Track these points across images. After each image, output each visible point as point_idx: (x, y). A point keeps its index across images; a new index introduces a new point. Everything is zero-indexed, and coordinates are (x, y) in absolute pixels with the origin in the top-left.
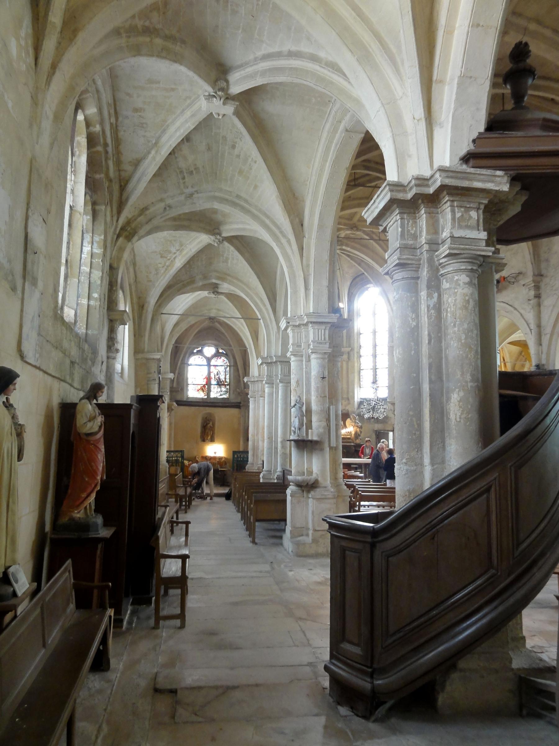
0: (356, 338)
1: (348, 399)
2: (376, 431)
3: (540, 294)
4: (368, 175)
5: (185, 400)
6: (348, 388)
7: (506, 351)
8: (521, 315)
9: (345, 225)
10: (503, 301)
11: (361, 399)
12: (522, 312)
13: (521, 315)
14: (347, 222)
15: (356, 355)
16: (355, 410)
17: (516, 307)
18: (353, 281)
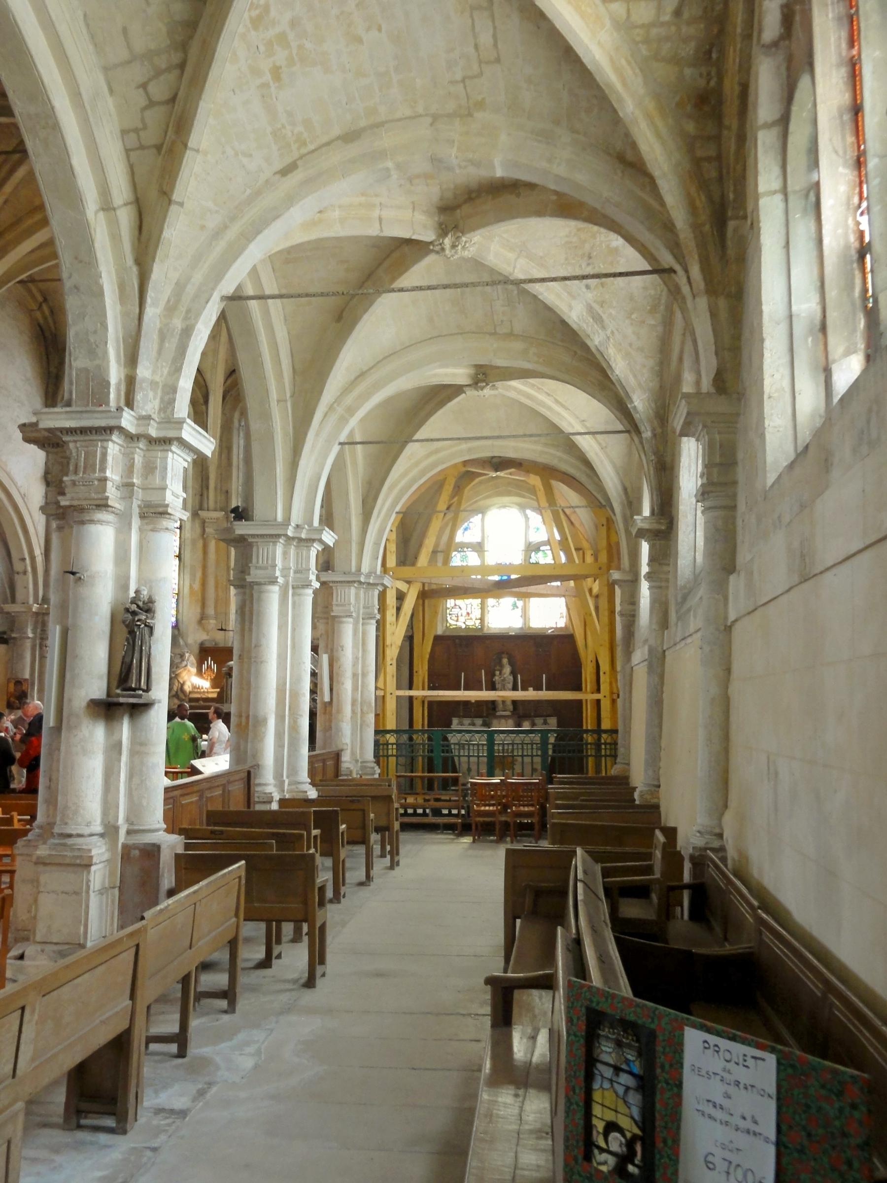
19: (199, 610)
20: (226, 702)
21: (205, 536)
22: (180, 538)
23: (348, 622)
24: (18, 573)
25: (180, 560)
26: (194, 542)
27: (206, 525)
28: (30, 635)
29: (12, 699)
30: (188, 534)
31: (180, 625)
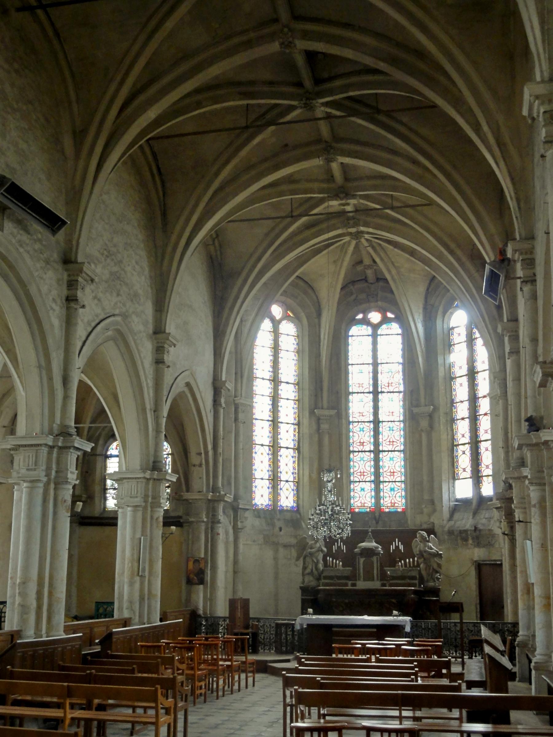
0: (442, 388)
1: (432, 502)
2: (476, 561)
3: (535, 275)
4: (276, 105)
5: (97, 515)
6: (431, 480)
11: (457, 500)
14: (325, 185)
15: (443, 420)
16: (445, 522)
18: (430, 284)
20: (359, 580)
21: (321, 431)
22: (299, 433)
24: (194, 466)
25: (299, 453)
26: (311, 436)
27: (321, 421)
28: (205, 520)
29: (192, 576)
30: (306, 430)
31: (301, 510)
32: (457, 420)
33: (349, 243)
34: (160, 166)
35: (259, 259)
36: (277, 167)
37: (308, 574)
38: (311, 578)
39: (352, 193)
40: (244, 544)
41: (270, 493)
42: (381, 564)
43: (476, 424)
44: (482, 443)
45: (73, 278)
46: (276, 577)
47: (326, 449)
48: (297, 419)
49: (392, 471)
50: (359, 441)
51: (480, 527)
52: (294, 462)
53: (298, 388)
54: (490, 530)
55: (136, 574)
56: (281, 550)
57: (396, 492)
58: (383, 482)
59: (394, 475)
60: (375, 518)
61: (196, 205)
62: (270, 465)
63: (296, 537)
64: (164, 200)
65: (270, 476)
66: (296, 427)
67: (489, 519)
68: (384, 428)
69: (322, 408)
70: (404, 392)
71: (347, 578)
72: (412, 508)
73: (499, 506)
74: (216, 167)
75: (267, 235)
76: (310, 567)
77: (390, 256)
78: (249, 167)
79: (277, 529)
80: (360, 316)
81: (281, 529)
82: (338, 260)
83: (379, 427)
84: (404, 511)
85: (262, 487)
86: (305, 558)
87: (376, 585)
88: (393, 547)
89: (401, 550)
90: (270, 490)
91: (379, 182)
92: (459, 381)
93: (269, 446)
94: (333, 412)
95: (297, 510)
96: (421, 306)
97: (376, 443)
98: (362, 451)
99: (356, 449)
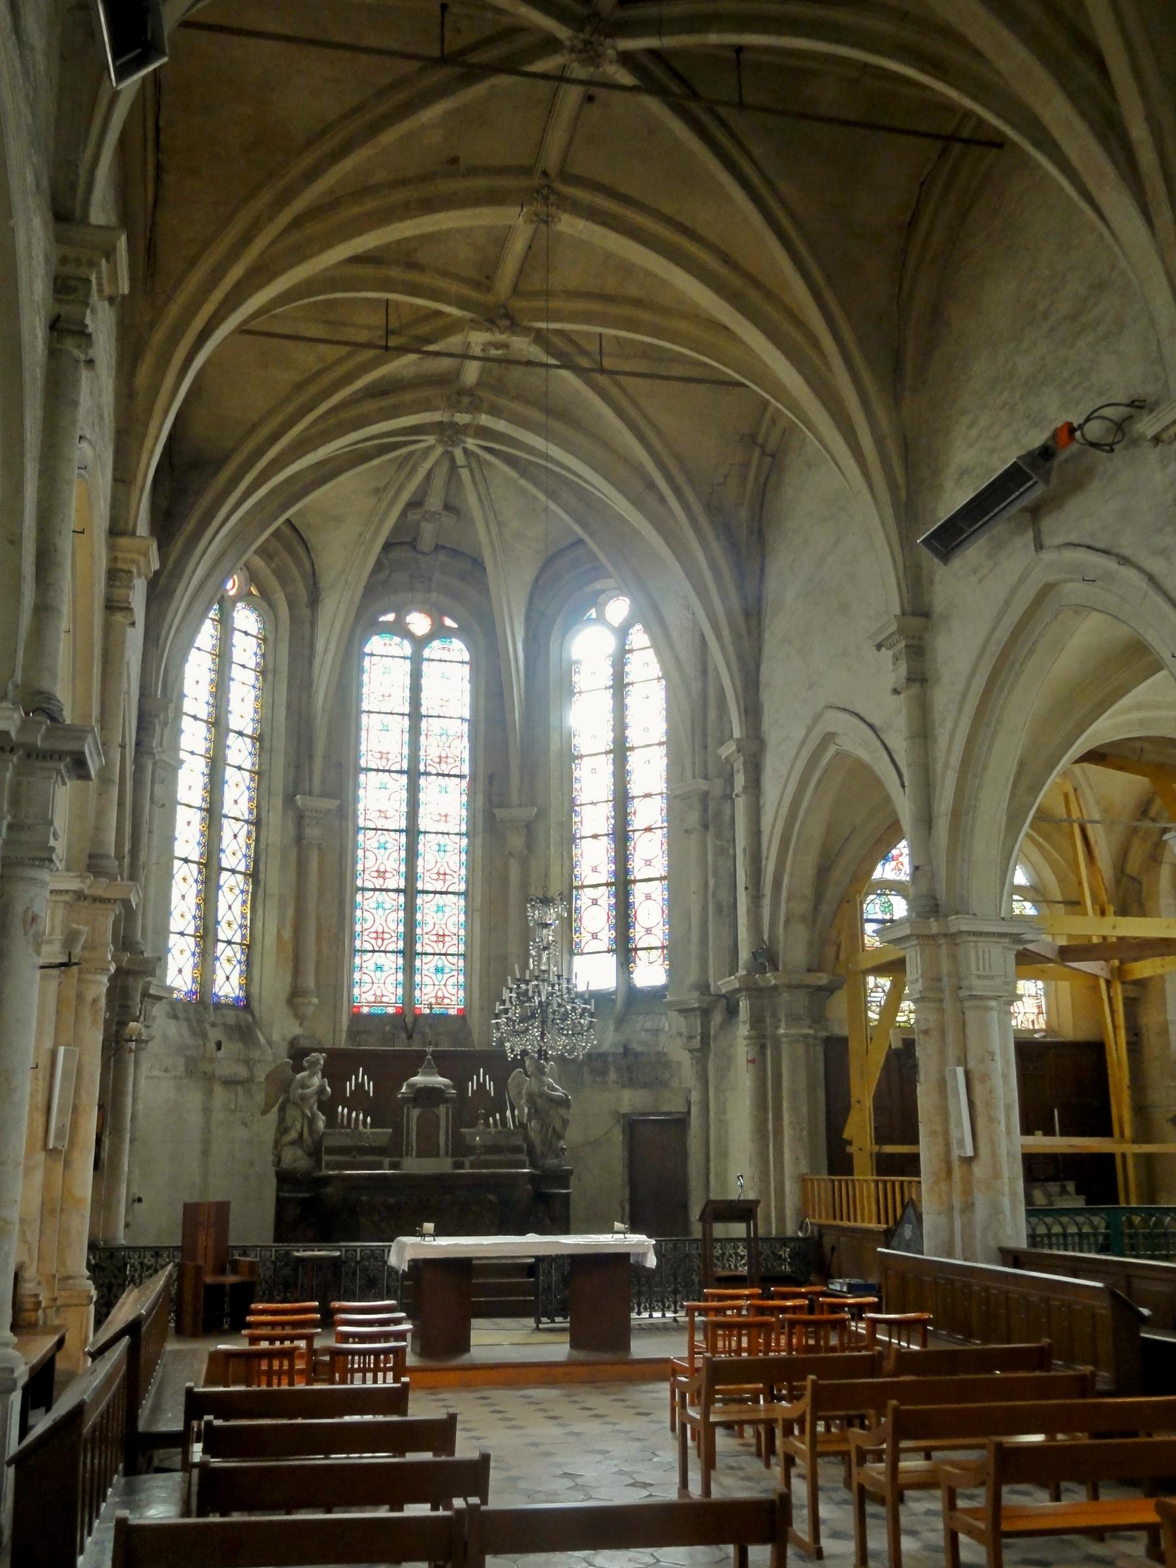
2: (624, 1115)
7: (1091, 800)
8: (1152, 579)
9: (463, 303)
10: (1073, 538)
12: (1156, 565)
13: (1152, 579)
15: (554, 836)
17: (1127, 551)
18: (542, 570)
19: (289, 979)
22: (257, 841)
23: (990, 1009)
26: (284, 851)
27: (307, 821)
30: (275, 835)
31: (255, 1005)
32: (582, 838)
33: (430, 449)
34: (162, 124)
35: (274, 438)
36: (428, 206)
37: (292, 1143)
38: (300, 1153)
39: (525, 323)
40: (147, 1077)
41: (195, 966)
42: (454, 1121)
43: (626, 848)
44: (638, 884)
45: (70, 269)
46: (206, 1153)
47: (313, 878)
48: (255, 810)
49: (441, 933)
50: (375, 868)
51: (635, 1046)
52: (244, 902)
53: (261, 748)
54: (660, 1054)
55: (40, 1144)
56: (218, 1089)
57: (446, 976)
58: (422, 954)
59: (443, 942)
60: (406, 1028)
61: (246, 239)
62: (198, 906)
63: (247, 1062)
64: (153, 216)
65: (197, 929)
66: (253, 828)
67: (656, 1032)
68: (426, 845)
69: (311, 794)
70: (474, 777)
71: (381, 1151)
72: (482, 1009)
73: (696, 1005)
74: (308, 160)
75: (299, 387)
76: (298, 1127)
77: (493, 496)
78: (364, 191)
79: (212, 1045)
80: (390, 617)
81: (219, 1046)
82: (385, 488)
83: (418, 843)
84: (462, 1016)
85: (182, 952)
86: (282, 1109)
87: (442, 1165)
88: (472, 1086)
89: (488, 1092)
90: (197, 959)
91: (595, 307)
92: (586, 763)
93: (199, 863)
94: (332, 804)
95: (246, 1004)
96: (523, 610)
97: (411, 875)
98: (381, 890)
99: (368, 885)
